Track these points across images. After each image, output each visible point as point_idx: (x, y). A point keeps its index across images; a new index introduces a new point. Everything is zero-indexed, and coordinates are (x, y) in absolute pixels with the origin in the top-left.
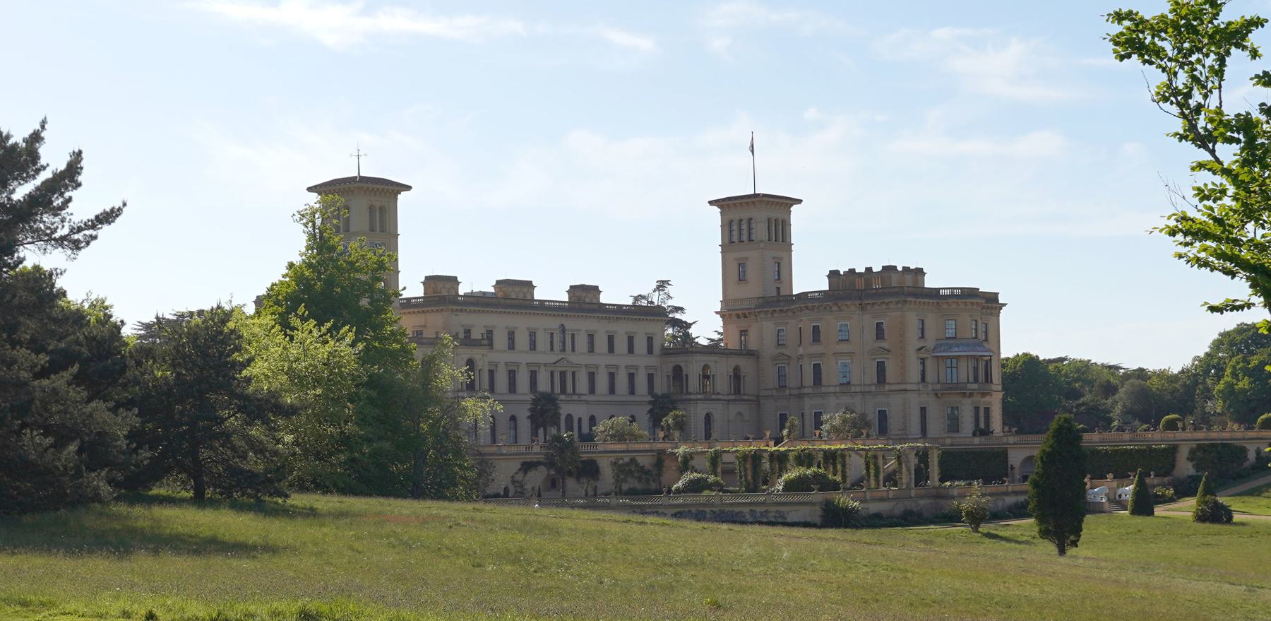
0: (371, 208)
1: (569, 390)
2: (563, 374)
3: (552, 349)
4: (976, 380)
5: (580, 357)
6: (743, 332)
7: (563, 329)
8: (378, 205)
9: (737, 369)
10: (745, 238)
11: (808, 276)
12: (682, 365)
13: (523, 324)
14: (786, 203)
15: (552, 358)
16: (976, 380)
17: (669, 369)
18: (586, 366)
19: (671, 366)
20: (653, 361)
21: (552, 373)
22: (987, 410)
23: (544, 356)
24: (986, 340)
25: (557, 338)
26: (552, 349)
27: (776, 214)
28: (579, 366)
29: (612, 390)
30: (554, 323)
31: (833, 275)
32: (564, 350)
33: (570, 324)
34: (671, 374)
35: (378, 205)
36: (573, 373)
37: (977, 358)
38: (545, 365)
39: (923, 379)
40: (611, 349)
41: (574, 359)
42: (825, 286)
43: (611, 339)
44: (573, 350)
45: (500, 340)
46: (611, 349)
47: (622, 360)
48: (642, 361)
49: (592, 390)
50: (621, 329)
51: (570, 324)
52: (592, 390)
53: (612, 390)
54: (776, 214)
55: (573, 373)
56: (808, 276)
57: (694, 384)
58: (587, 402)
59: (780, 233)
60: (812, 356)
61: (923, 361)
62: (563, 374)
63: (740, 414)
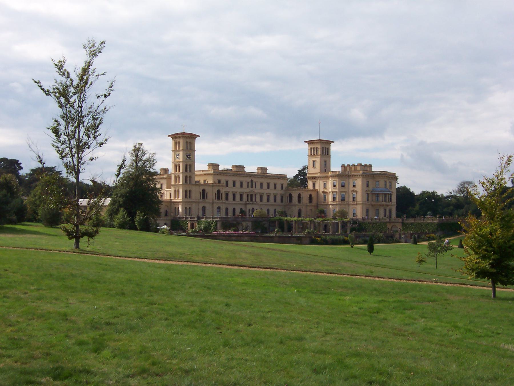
0: (187, 142)
1: (254, 200)
2: (252, 196)
4: (385, 201)
5: (258, 190)
6: (314, 184)
7: (252, 180)
8: (189, 141)
9: (311, 195)
10: (315, 153)
11: (335, 167)
13: (238, 180)
14: (329, 143)
15: (248, 190)
16: (385, 201)
20: (282, 192)
21: (248, 195)
22: (390, 211)
23: (245, 190)
24: (391, 188)
27: (325, 146)
29: (268, 201)
31: (343, 166)
32: (252, 187)
33: (254, 180)
35: (189, 141)
37: (385, 194)
39: (368, 200)
40: (268, 187)
41: (256, 191)
42: (340, 169)
43: (275, 185)
45: (231, 184)
46: (268, 187)
47: (272, 191)
48: (279, 192)
49: (261, 200)
50: (272, 182)
52: (261, 200)
53: (268, 201)
54: (325, 146)
56: (335, 167)
57: (295, 200)
59: (326, 152)
60: (333, 192)
61: (368, 194)
62: (252, 196)
63: (311, 209)
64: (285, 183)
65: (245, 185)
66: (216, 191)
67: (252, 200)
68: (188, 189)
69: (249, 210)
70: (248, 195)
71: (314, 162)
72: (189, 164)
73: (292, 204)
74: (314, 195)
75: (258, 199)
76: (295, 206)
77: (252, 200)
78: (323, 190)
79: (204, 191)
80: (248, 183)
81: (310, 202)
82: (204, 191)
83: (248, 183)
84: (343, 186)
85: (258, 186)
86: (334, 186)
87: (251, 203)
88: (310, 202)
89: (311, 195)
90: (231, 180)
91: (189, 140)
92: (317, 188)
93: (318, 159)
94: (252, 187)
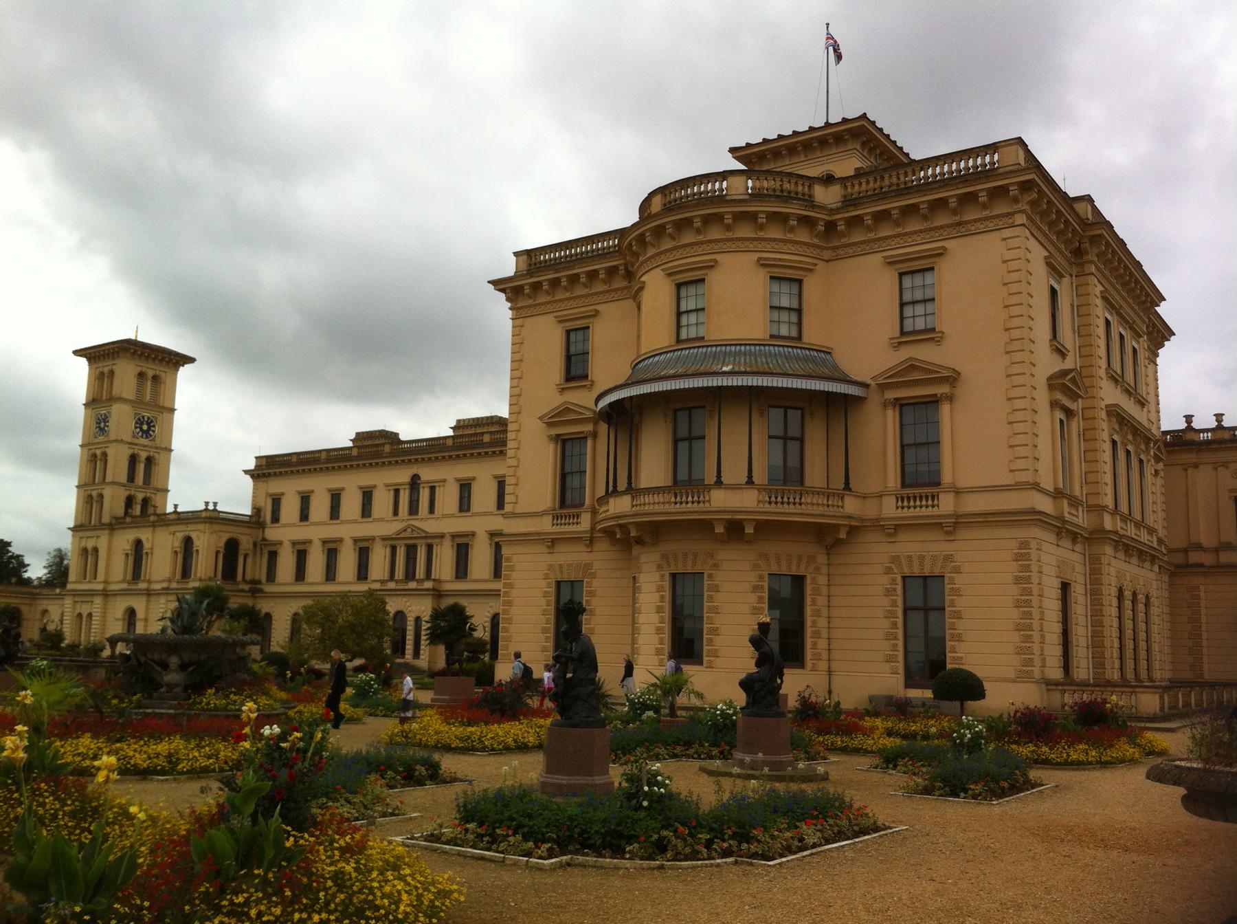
0: (141, 375)
2: (411, 550)
3: (396, 513)
5: (444, 520)
8: (106, 370)
15: (392, 528)
18: (454, 536)
23: (384, 524)
26: (396, 513)
28: (442, 536)
30: (402, 476)
32: (413, 509)
35: (106, 370)
38: (384, 539)
41: (431, 526)
44: (432, 510)
51: (428, 474)
55: (430, 548)
58: (438, 594)
62: (411, 550)
64: (533, 468)
65: (382, 503)
66: (177, 544)
67: (410, 575)
68: (90, 545)
69: (418, 619)
70: (394, 549)
72: (144, 455)
77: (410, 575)
79: (138, 544)
80: (397, 492)
82: (138, 544)
83: (397, 492)
85: (448, 498)
90: (320, 486)
91: (106, 366)
94: (413, 509)
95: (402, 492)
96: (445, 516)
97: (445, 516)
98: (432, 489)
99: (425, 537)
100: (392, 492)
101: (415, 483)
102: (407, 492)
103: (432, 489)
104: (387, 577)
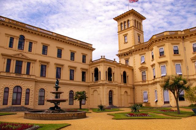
10: (126, 27)
12: (98, 67)
15: (11, 52)
17: (92, 70)
18: (39, 61)
19: (93, 68)
21: (9, 61)
25: (16, 43)
28: (35, 61)
30: (17, 34)
33: (27, 36)
34: (94, 72)
36: (29, 65)
41: (30, 56)
51: (27, 36)
55: (29, 65)
58: (36, 82)
70: (9, 61)
71: (125, 36)
73: (100, 82)
74: (128, 73)
75: (36, 70)
76: (103, 85)
78: (140, 66)
80: (12, 40)
81: (125, 82)
83: (12, 40)
84: (176, 52)
85: (38, 48)
86: (162, 54)
87: (26, 76)
88: (125, 82)
89: (125, 73)
92: (131, 64)
93: (130, 33)
95: (15, 40)
96: (36, 54)
97: (36, 54)
98: (31, 44)
99: (28, 59)
100: (9, 39)
101: (22, 38)
102: (18, 41)
103: (31, 44)
104: (5, 70)
